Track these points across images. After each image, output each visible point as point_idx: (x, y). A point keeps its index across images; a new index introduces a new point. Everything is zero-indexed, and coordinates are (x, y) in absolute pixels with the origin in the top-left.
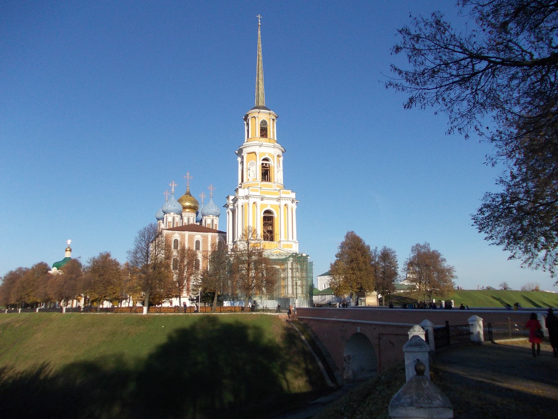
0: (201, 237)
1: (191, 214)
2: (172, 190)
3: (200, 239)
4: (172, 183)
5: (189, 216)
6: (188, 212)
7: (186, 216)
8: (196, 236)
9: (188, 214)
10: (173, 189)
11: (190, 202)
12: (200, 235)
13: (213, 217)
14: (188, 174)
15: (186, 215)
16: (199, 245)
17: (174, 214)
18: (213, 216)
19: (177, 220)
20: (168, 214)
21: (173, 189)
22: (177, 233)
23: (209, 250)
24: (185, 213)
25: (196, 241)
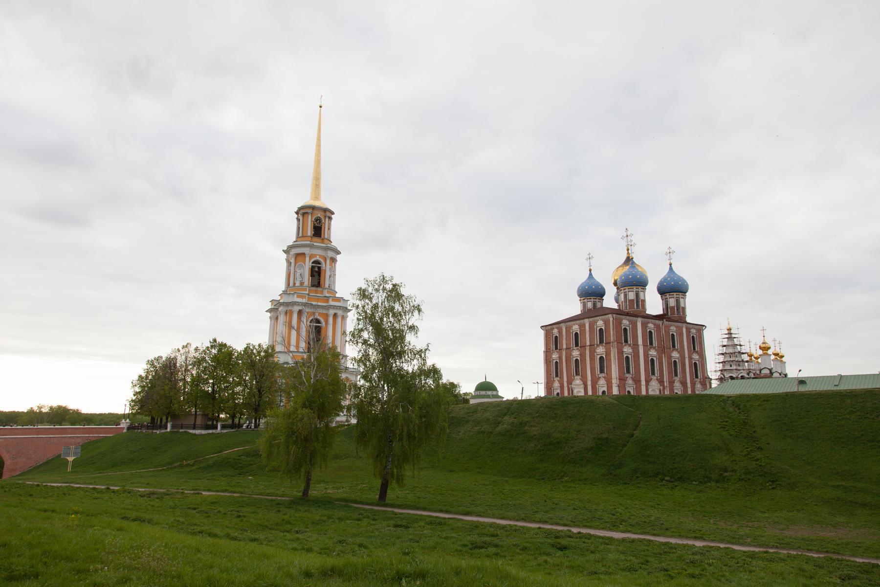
13: (625, 291)
19: (588, 306)
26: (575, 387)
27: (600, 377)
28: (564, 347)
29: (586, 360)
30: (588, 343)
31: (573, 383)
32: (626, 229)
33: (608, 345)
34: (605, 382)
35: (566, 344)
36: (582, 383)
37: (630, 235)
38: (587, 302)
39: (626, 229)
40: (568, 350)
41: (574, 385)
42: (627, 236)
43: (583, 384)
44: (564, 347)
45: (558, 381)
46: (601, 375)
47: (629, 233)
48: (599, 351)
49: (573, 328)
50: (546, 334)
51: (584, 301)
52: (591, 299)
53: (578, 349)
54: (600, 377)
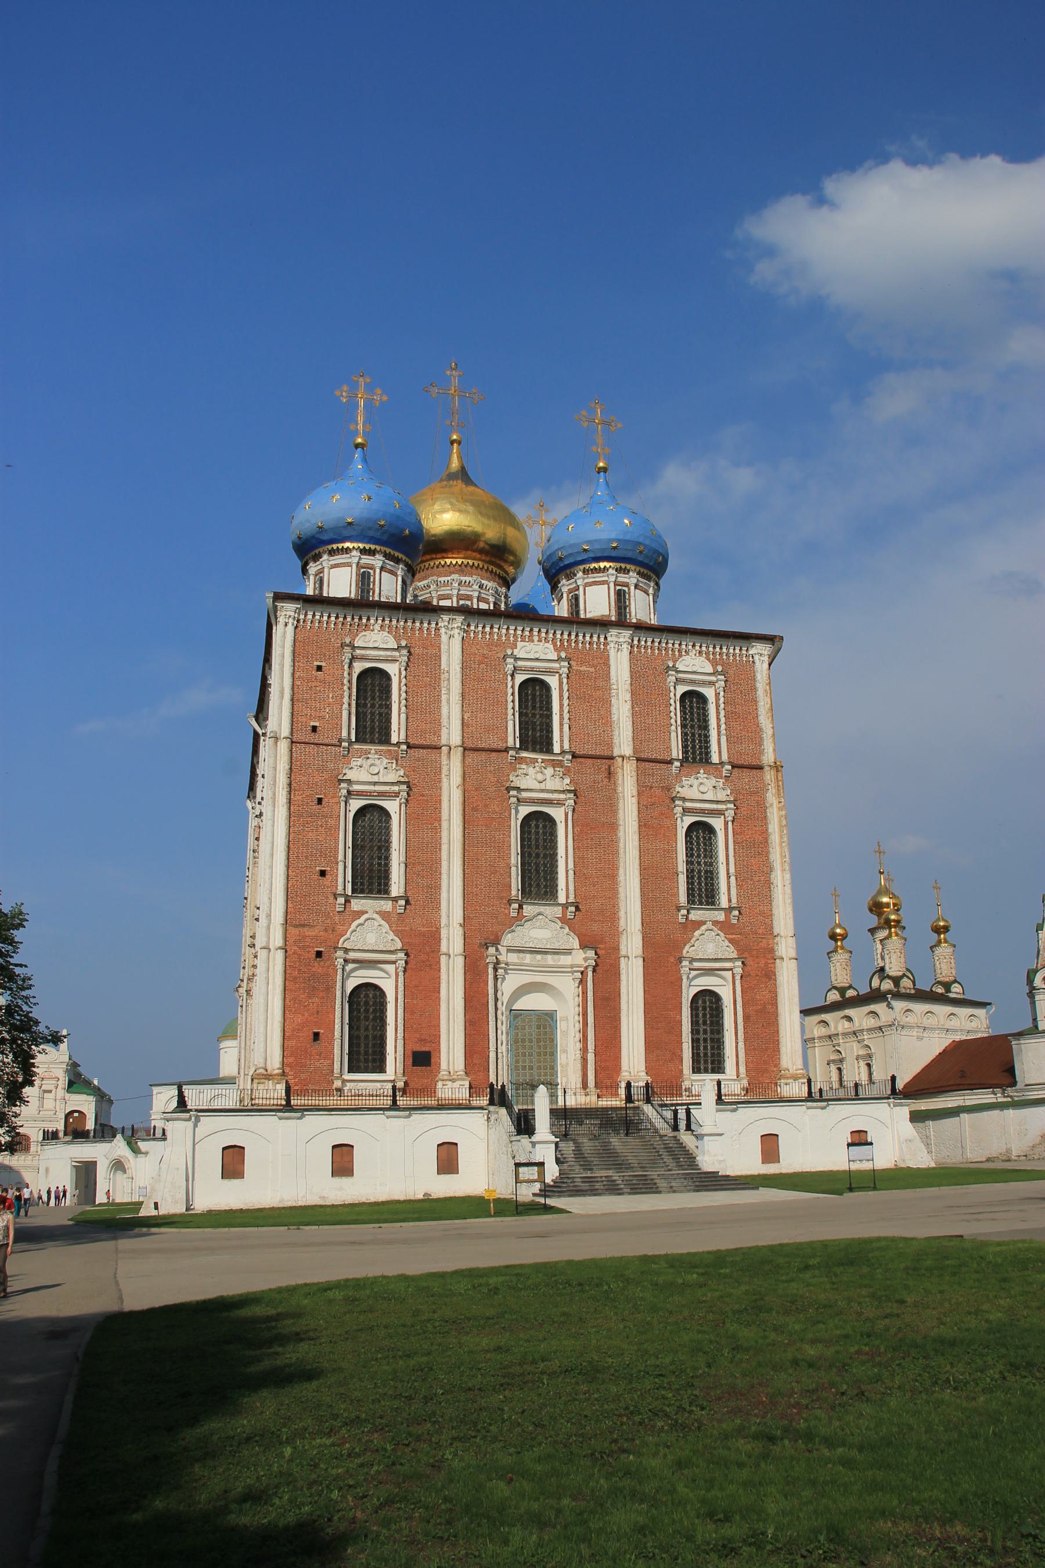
2: (357, 424)
4: (354, 387)
5: (469, 598)
6: (461, 569)
10: (360, 419)
11: (471, 509)
12: (550, 646)
13: (623, 578)
14: (454, 377)
16: (549, 717)
17: (364, 552)
18: (626, 571)
20: (325, 557)
21: (360, 419)
22: (377, 627)
23: (616, 753)
24: (442, 579)
25: (524, 685)
26: (513, 958)
27: (700, 924)
28: (452, 733)
29: (613, 827)
30: (623, 743)
31: (508, 939)
34: (731, 952)
40: (472, 757)
41: (508, 951)
43: (583, 946)
44: (452, 733)
45: (385, 915)
48: (694, 793)
52: (397, 561)
53: (555, 764)
54: (700, 924)
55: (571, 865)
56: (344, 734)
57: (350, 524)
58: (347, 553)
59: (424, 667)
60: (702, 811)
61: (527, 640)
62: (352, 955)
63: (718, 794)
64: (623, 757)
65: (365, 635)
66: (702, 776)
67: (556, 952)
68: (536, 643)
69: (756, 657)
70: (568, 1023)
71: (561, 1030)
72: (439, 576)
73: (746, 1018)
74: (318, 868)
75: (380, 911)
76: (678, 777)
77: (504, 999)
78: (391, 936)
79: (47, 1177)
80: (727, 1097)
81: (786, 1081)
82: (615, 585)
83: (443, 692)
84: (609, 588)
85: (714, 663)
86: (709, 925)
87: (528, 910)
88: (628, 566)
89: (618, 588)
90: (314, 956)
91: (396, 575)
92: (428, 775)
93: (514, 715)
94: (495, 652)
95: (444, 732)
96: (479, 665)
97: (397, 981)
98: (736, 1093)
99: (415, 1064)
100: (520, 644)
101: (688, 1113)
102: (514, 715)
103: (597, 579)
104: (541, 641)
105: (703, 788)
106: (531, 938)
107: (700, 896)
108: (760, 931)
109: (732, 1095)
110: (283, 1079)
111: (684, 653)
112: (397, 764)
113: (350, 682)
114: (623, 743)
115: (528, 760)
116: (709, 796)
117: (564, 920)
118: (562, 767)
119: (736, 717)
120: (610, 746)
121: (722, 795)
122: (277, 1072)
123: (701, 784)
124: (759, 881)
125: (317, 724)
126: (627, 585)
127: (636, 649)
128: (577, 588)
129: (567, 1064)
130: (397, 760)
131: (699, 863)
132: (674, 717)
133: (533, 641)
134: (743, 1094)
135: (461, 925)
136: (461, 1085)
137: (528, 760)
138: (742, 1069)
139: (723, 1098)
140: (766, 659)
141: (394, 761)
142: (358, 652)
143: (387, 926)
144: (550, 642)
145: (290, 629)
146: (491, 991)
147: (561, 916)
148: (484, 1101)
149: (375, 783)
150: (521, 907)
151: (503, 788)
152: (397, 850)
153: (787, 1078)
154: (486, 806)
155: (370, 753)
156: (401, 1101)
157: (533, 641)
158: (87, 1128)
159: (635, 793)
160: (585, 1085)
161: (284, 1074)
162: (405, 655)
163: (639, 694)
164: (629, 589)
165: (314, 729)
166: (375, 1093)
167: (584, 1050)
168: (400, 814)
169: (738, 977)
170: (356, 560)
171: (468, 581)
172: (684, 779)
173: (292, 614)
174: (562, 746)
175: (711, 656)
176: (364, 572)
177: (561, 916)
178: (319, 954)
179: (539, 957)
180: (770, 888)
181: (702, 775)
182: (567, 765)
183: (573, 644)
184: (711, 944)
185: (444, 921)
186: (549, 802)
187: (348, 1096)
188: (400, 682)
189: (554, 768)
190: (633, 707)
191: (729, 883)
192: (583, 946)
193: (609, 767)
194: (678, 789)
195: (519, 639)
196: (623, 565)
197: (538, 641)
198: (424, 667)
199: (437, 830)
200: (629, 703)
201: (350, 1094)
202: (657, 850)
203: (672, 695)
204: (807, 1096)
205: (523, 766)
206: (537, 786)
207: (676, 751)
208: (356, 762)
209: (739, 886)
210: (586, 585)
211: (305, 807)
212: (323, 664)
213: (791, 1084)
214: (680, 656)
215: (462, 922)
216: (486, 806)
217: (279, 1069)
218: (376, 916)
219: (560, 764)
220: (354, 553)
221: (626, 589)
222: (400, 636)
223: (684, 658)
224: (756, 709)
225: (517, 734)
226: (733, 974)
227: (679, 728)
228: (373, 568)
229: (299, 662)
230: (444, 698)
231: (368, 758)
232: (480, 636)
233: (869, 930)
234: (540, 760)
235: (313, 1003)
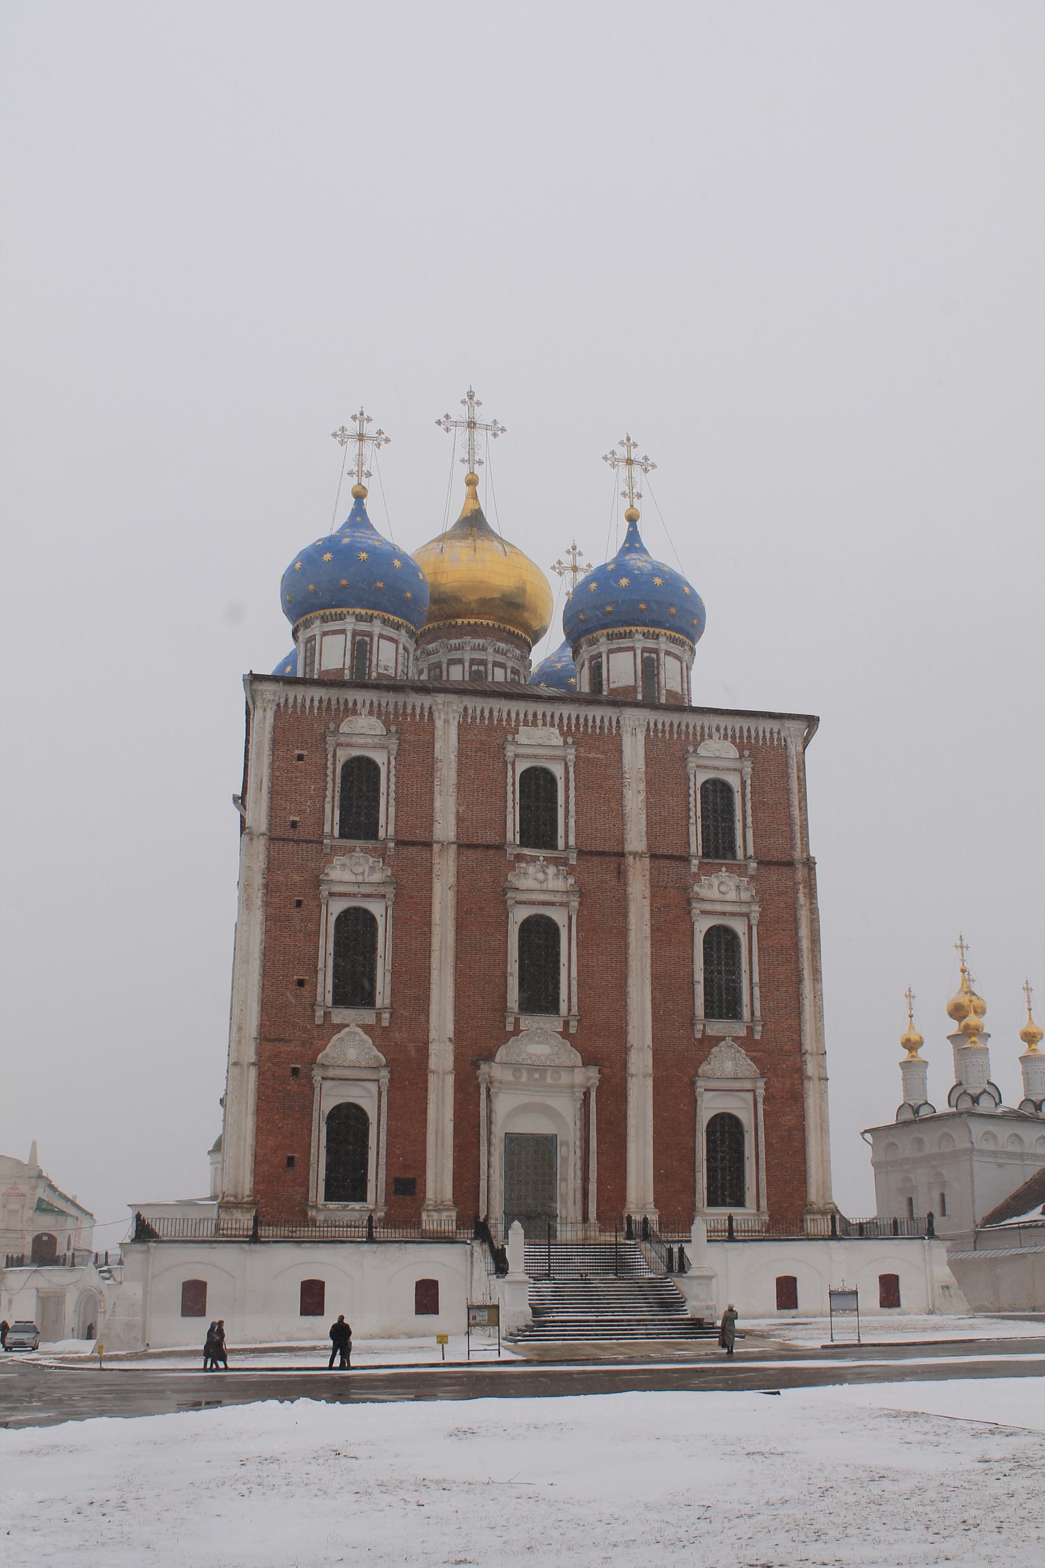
0: (559, 741)
1: (490, 650)
3: (552, 758)
5: (483, 662)
7: (460, 661)
8: (525, 735)
9: (473, 649)
12: (556, 731)
13: (651, 644)
15: (456, 655)
16: (555, 810)
17: (359, 618)
20: (317, 623)
24: (454, 642)
26: (507, 1075)
27: (718, 1040)
29: (623, 933)
30: (636, 840)
32: (471, 396)
33: (774, 875)
35: (460, 819)
36: (577, 1058)
37: (487, 428)
38: (381, 636)
39: (471, 396)
42: (472, 425)
43: (586, 1063)
45: (367, 1029)
46: (717, 1027)
47: (482, 416)
48: (714, 894)
49: (521, 738)
50: (275, 727)
51: (363, 626)
53: (556, 862)
54: (718, 1040)
55: (574, 973)
56: (327, 829)
57: (344, 587)
58: (341, 619)
59: (416, 756)
60: (724, 914)
61: (530, 724)
62: (331, 1073)
63: (742, 894)
64: (635, 854)
65: (351, 721)
66: (724, 875)
67: (557, 1068)
68: (540, 727)
69: (789, 740)
70: (568, 1148)
71: (561, 1157)
72: (449, 639)
73: (769, 1145)
74: (295, 977)
75: (363, 1025)
76: (696, 878)
77: (499, 1117)
78: (375, 1052)
79: (9, 1310)
80: (739, 1234)
81: (812, 1217)
82: (642, 653)
83: (436, 783)
84: (635, 655)
85: (741, 748)
86: (729, 1040)
87: (528, 1022)
88: (657, 631)
89: (646, 655)
90: (289, 1072)
91: (396, 642)
92: (417, 875)
93: (514, 808)
94: (494, 738)
95: (437, 828)
96: (476, 752)
97: (380, 1101)
98: (757, 1229)
99: (397, 1191)
100: (520, 728)
101: (681, 1250)
102: (514, 808)
103: (622, 646)
104: (546, 725)
105: (723, 888)
106: (528, 1054)
107: (720, 1007)
108: (786, 1048)
109: (752, 1231)
110: (254, 1208)
111: (706, 737)
112: (383, 862)
113: (334, 772)
114: (636, 840)
115: (528, 858)
116: (732, 896)
117: (565, 1034)
118: (566, 865)
119: (764, 808)
120: (622, 840)
121: (745, 896)
122: (246, 1199)
123: (722, 883)
124: (786, 991)
125: (297, 819)
126: (656, 651)
127: (652, 734)
128: (600, 655)
129: (567, 1194)
130: (383, 860)
131: (720, 972)
132: (694, 809)
133: (537, 726)
134: (764, 1230)
135: (450, 1040)
136: (447, 1216)
137: (528, 858)
138: (764, 1203)
139: (735, 1234)
140: (800, 741)
141: (381, 860)
142: (342, 739)
143: (370, 1041)
144: (556, 727)
145: (270, 715)
146: (483, 1113)
147: (562, 1030)
148: (470, 1233)
149: (359, 884)
150: (517, 1020)
151: (499, 890)
152: (383, 957)
153: (814, 1213)
154: (481, 909)
155: (354, 851)
156: (379, 1233)
157: (537, 726)
158: (57, 1254)
159: (648, 894)
160: (585, 1218)
161: (254, 1203)
162: (395, 743)
163: (655, 783)
164: (658, 656)
165: (294, 824)
166: (353, 1224)
167: (585, 1179)
168: (386, 918)
169: (760, 1100)
170: (350, 628)
171: (481, 644)
172: (703, 878)
173: (271, 697)
174: (567, 843)
175: (738, 740)
176: (359, 642)
177: (562, 1030)
178: (295, 1071)
179: (537, 1075)
180: (799, 1000)
181: (724, 873)
182: (571, 863)
183: (582, 729)
184: (730, 1063)
185: (433, 1035)
186: (553, 904)
187: (319, 1227)
188: (389, 773)
189: (557, 866)
190: (647, 798)
191: (752, 994)
192: (586, 1063)
193: (619, 865)
194: (696, 889)
195: (522, 724)
196: (651, 630)
197: (543, 725)
198: (416, 756)
199: (427, 934)
200: (643, 795)
201: (325, 1225)
202: (670, 957)
203: (692, 784)
204: (830, 1234)
205: (523, 865)
206: (538, 886)
207: (696, 845)
208: (337, 860)
209: (763, 997)
210: (610, 651)
211: (282, 910)
212: (305, 753)
213: (819, 1220)
214: (703, 739)
215: (452, 1036)
216: (481, 909)
217: (249, 1196)
218: (359, 1030)
219: (564, 861)
220: (350, 620)
221: (654, 656)
222: (389, 720)
223: (707, 742)
224: (788, 799)
225: (518, 829)
226: (755, 1096)
227: (699, 821)
228: (370, 635)
229: (278, 750)
230: (437, 788)
231: (352, 856)
232: (478, 720)
233: (948, 1037)
234: (541, 858)
235: (288, 1124)
